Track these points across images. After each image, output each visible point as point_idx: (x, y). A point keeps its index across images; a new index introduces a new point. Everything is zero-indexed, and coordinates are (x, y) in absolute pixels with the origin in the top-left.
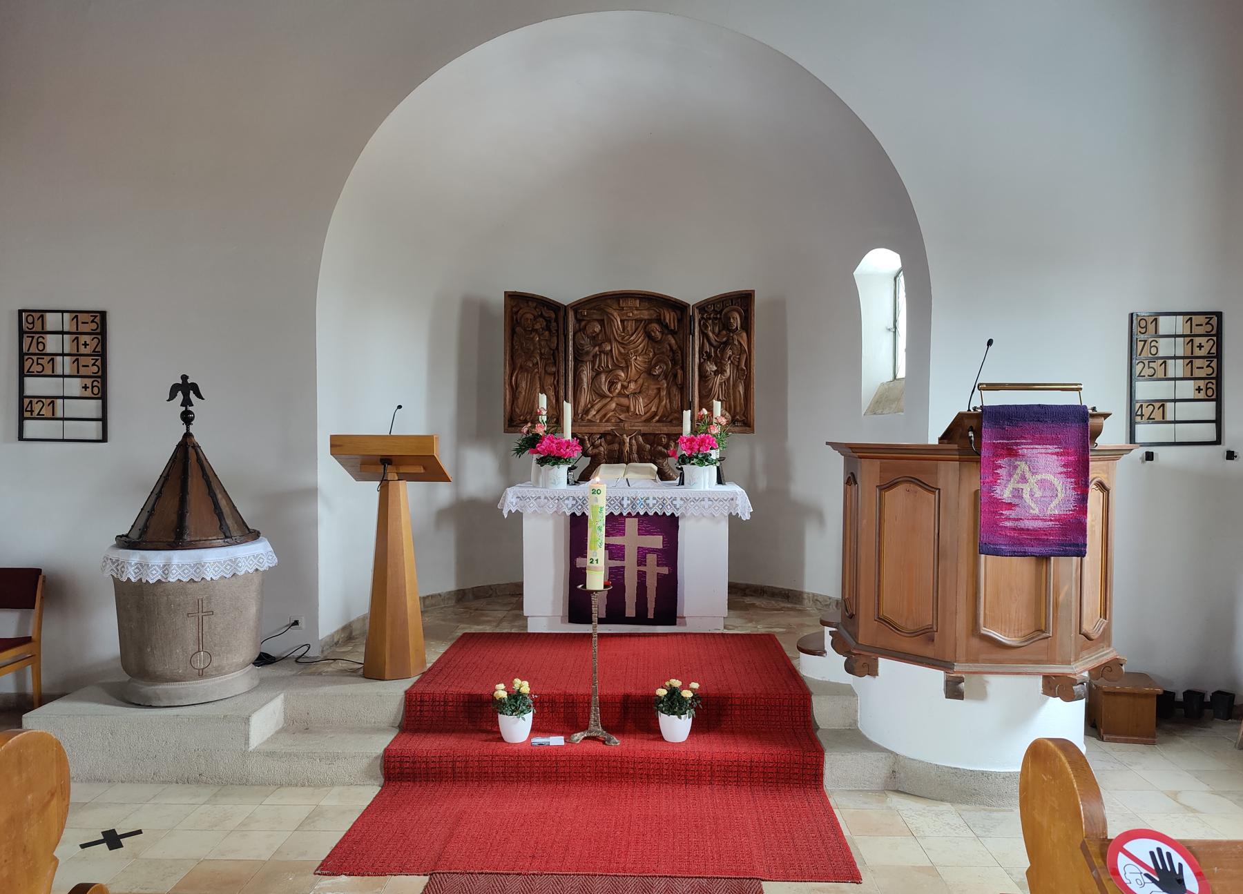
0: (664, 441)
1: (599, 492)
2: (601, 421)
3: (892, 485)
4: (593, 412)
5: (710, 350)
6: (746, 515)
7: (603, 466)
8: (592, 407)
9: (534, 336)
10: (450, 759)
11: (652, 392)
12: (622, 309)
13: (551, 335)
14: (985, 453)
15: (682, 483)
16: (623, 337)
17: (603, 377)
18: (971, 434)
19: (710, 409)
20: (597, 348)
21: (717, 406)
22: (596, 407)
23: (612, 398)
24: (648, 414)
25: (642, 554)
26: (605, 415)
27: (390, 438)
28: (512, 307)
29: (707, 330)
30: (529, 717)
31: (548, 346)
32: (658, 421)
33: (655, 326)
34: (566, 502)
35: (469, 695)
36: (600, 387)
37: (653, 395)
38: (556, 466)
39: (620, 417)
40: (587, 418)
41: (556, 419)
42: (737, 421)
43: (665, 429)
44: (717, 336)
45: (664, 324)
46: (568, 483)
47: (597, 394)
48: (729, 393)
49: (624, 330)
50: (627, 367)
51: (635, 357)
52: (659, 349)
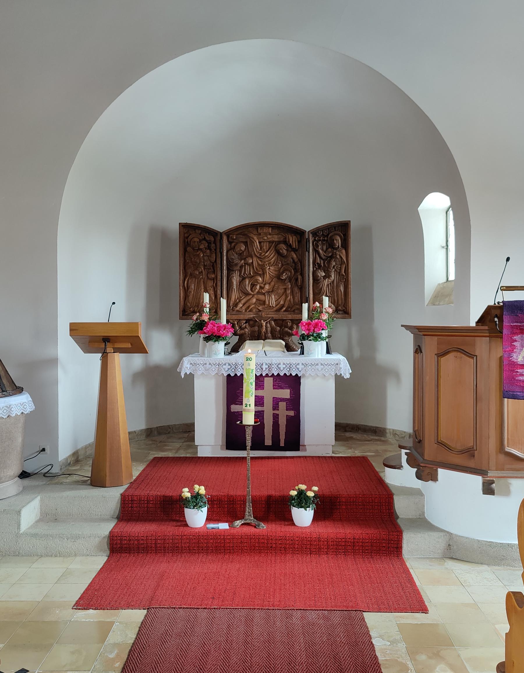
0: (289, 324)
1: (251, 359)
2: (246, 311)
3: (445, 354)
4: (240, 305)
5: (320, 262)
6: (347, 375)
7: (248, 342)
8: (240, 301)
9: (200, 253)
10: (153, 538)
11: (281, 291)
12: (260, 234)
13: (211, 252)
14: (505, 331)
15: (302, 353)
16: (261, 253)
17: (247, 281)
18: (496, 319)
19: (321, 302)
20: (243, 261)
21: (326, 300)
22: (243, 302)
23: (253, 295)
24: (278, 306)
25: (276, 402)
26: (249, 307)
27: (108, 324)
28: (184, 234)
30: (205, 510)
31: (209, 260)
32: (285, 311)
35: (164, 496)
36: (245, 288)
37: (282, 293)
38: (217, 342)
39: (259, 308)
41: (215, 311)
42: (340, 310)
43: (290, 317)
44: (325, 252)
45: (289, 244)
46: (225, 354)
48: (333, 291)
49: (261, 248)
50: (264, 274)
51: (269, 267)
52: (285, 262)
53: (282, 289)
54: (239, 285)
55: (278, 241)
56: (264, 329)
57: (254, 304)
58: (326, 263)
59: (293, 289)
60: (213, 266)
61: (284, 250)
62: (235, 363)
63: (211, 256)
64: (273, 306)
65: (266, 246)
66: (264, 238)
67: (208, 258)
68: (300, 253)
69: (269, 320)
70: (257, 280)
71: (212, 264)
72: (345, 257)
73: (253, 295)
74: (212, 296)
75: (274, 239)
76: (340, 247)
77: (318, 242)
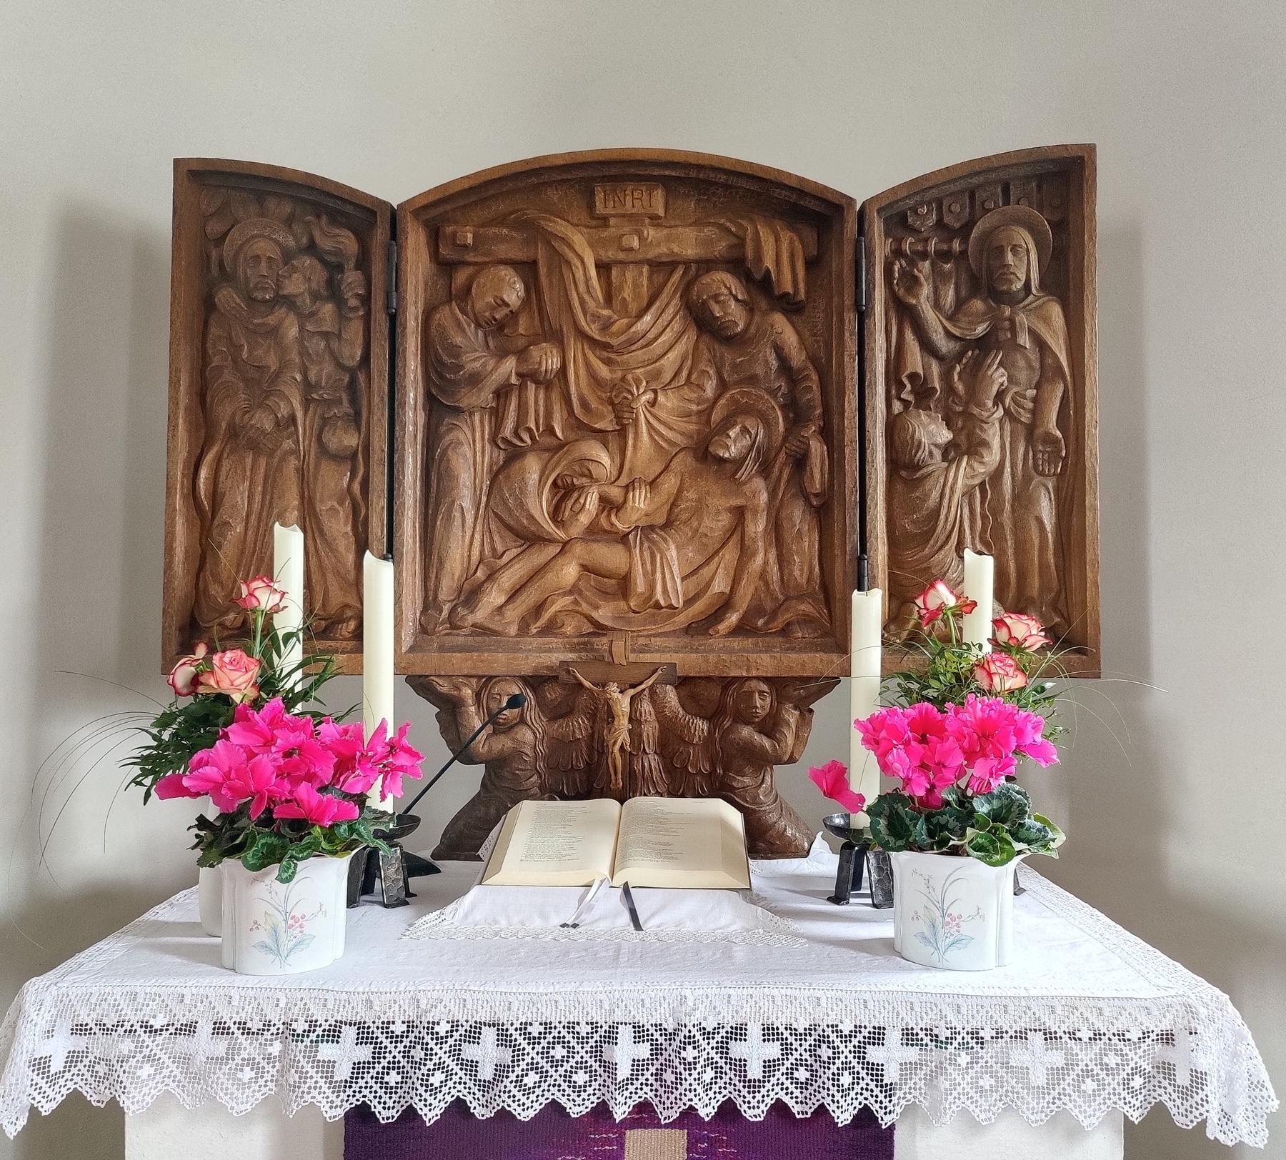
0: (762, 704)
4: (494, 597)
7: (527, 809)
8: (491, 577)
9: (281, 322)
11: (716, 524)
16: (606, 326)
17: (532, 467)
20: (510, 364)
22: (509, 579)
23: (565, 544)
24: (699, 606)
26: (539, 608)
29: (916, 296)
32: (738, 631)
33: (724, 283)
34: (327, 1051)
36: (521, 505)
38: (275, 869)
39: (595, 615)
40: (470, 619)
45: (758, 276)
47: (509, 528)
48: (998, 527)
49: (609, 299)
50: (622, 433)
51: (650, 396)
53: (718, 512)
54: (491, 487)
55: (696, 262)
56: (621, 734)
57: (570, 592)
58: (956, 377)
59: (778, 512)
60: (352, 387)
61: (733, 303)
62: (411, 1026)
63: (339, 336)
64: (671, 607)
65: (636, 286)
66: (625, 242)
67: (328, 346)
68: (820, 317)
69: (650, 681)
70: (583, 460)
71: (347, 379)
72: (1062, 341)
73: (565, 546)
74: (342, 549)
75: (676, 250)
76: (1034, 290)
77: (912, 263)
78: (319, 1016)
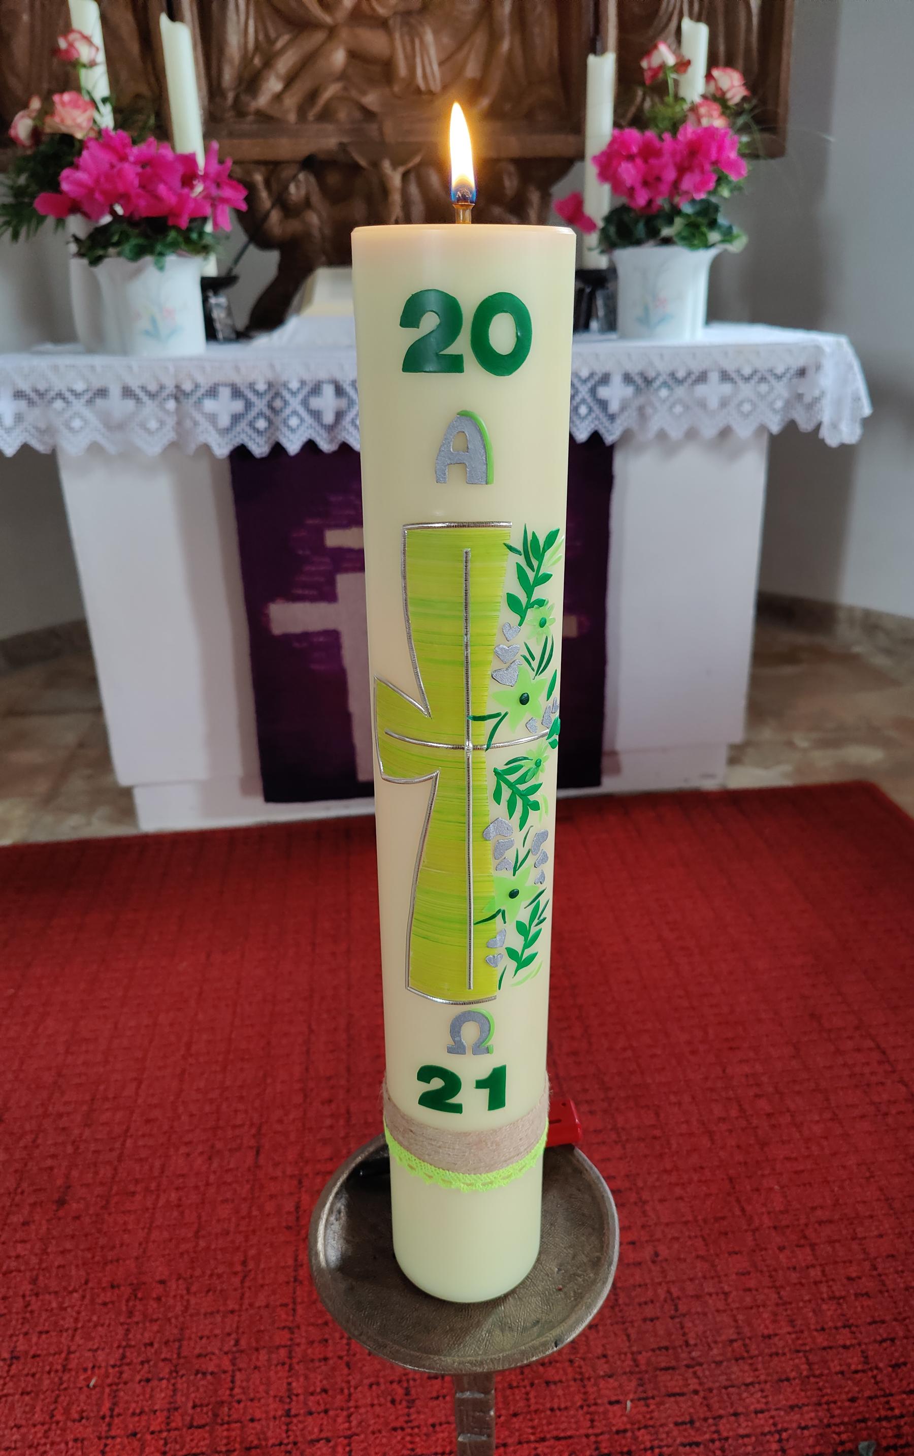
4: (273, 84)
8: (268, 63)
22: (284, 64)
26: (313, 96)
34: (209, 405)
38: (148, 259)
46: (211, 333)
73: (332, 31)
78: (201, 379)
